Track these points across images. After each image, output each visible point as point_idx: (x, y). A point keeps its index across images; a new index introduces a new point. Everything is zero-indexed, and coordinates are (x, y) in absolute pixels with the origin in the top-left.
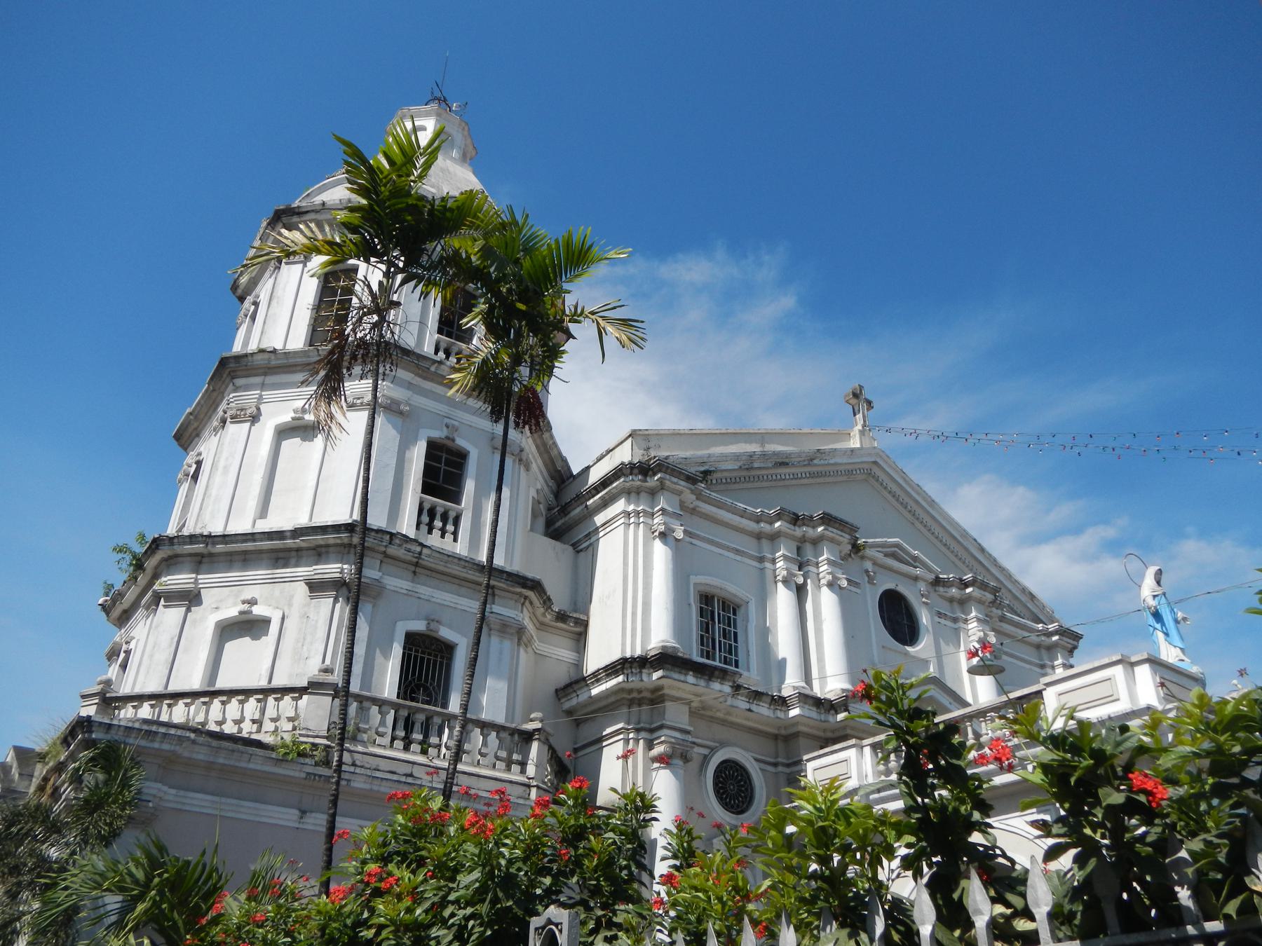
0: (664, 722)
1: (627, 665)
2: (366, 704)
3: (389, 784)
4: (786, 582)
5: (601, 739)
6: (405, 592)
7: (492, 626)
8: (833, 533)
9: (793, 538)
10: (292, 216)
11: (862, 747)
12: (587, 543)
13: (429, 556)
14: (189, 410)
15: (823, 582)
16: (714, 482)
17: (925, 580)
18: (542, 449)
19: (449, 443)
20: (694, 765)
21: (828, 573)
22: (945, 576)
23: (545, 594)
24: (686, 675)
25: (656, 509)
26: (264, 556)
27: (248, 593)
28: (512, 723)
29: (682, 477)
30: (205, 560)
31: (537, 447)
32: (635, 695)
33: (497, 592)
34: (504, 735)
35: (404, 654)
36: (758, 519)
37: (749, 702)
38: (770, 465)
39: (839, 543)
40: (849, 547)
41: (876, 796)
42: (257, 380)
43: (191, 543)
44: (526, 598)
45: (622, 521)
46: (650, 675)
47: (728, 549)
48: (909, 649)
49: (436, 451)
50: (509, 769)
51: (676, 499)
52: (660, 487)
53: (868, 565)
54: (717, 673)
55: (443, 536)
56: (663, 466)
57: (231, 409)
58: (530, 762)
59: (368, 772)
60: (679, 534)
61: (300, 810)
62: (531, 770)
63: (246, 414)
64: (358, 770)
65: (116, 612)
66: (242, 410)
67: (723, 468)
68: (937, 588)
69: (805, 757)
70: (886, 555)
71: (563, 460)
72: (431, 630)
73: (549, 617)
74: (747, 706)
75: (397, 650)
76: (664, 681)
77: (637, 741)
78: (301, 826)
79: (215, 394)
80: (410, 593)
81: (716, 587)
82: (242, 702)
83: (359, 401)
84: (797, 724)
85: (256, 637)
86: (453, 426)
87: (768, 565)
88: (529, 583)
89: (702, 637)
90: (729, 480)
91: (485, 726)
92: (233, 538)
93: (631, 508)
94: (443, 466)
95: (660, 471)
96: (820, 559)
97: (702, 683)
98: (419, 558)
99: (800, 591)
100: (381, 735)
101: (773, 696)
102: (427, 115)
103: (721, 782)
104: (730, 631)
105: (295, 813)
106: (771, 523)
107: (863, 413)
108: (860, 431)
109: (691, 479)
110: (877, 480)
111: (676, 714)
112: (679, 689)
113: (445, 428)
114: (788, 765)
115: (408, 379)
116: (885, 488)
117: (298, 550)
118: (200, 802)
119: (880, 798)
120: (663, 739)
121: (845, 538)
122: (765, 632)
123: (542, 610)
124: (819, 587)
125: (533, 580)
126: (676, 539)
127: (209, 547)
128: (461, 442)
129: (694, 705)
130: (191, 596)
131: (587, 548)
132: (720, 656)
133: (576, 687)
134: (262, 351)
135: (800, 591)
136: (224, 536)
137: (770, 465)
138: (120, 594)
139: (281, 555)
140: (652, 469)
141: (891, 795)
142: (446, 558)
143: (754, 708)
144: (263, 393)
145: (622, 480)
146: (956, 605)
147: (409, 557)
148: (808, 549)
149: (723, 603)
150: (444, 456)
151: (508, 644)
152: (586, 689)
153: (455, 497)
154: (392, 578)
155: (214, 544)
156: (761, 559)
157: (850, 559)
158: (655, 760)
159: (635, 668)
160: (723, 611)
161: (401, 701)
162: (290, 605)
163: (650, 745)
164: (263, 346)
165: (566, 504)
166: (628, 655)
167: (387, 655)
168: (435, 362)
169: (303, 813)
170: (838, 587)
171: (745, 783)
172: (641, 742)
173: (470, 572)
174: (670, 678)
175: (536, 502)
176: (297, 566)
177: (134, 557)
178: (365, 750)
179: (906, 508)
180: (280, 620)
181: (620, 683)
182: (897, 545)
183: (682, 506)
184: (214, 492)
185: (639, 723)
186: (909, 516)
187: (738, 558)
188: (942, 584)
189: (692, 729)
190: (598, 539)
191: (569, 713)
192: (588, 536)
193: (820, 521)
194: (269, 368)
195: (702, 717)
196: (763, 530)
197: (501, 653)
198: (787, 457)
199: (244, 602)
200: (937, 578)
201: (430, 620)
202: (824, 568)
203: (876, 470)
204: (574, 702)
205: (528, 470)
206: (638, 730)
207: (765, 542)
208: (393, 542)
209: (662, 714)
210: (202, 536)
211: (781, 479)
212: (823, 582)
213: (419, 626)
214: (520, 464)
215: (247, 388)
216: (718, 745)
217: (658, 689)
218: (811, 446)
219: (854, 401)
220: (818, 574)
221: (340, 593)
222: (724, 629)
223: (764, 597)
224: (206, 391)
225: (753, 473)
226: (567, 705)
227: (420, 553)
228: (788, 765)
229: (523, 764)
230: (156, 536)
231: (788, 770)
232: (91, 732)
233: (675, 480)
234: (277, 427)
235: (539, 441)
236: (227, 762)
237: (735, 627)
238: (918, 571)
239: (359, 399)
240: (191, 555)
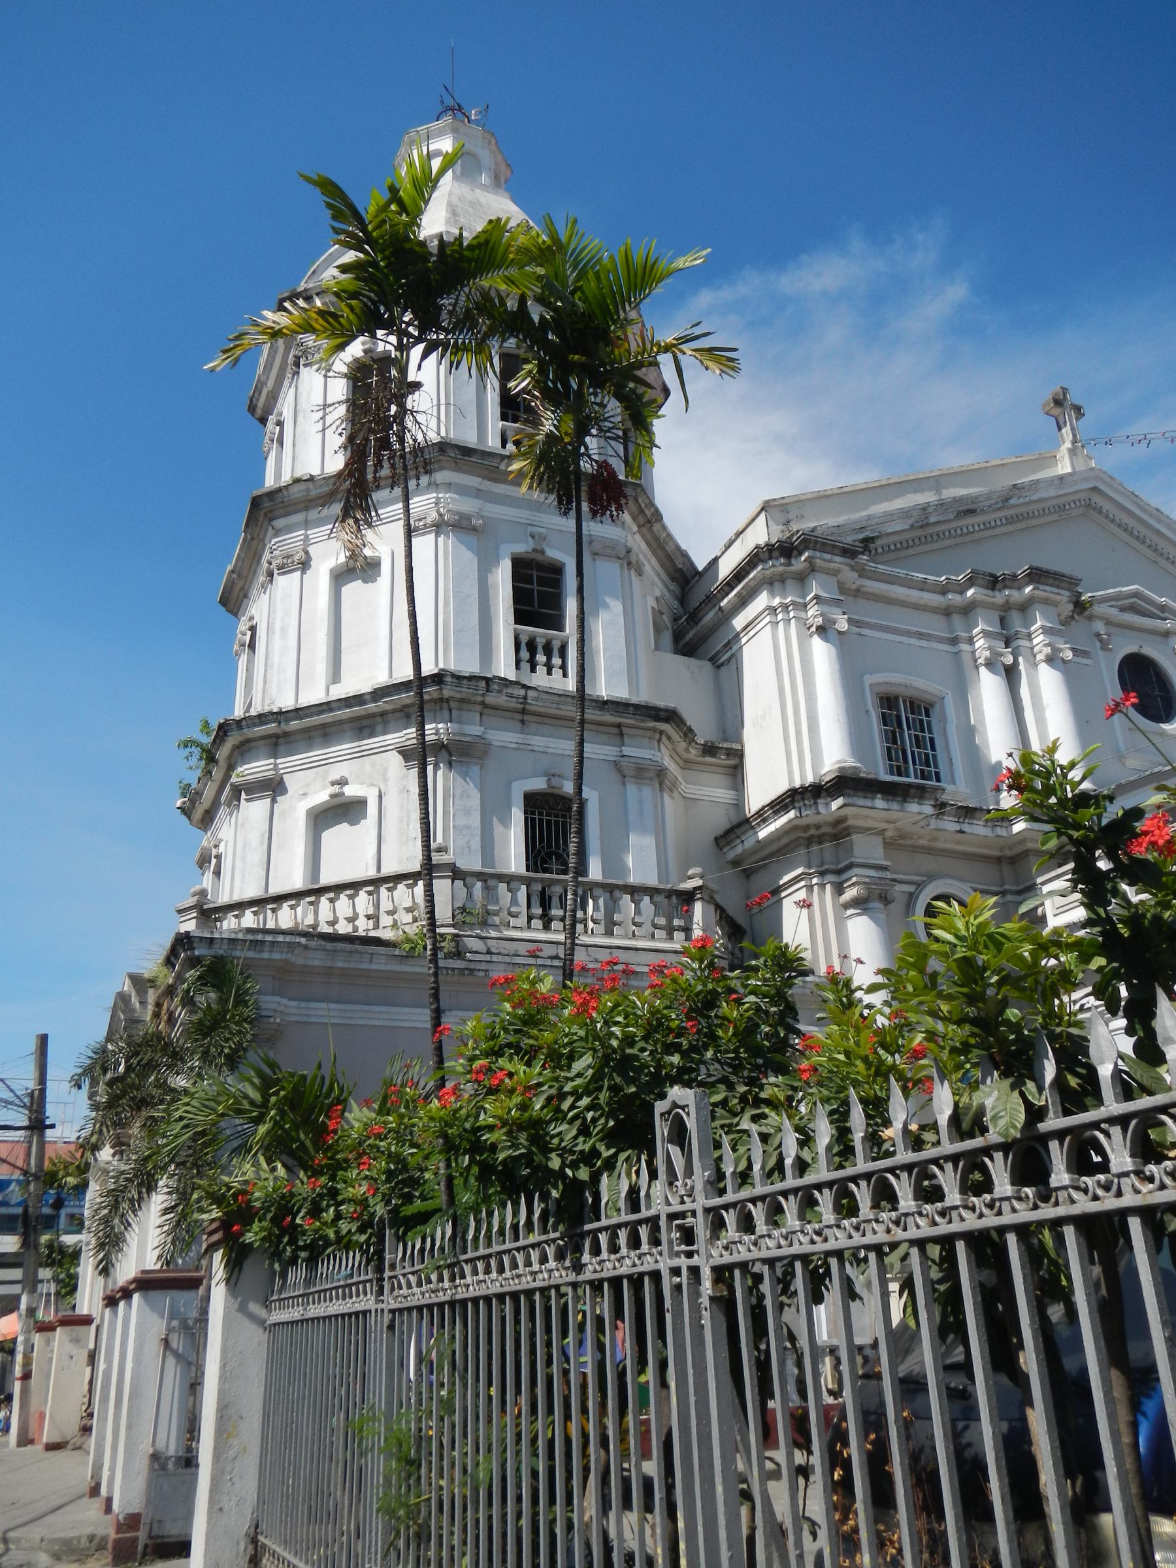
0: (853, 860)
1: (798, 797)
2: (491, 882)
4: (989, 665)
5: (777, 891)
6: (515, 746)
7: (626, 772)
8: (1045, 592)
9: (992, 606)
13: (536, 699)
14: (229, 568)
15: (1040, 657)
16: (880, 550)
18: (655, 545)
20: (897, 907)
21: (1046, 645)
23: (685, 724)
24: (873, 799)
25: (808, 598)
26: (346, 726)
27: (336, 772)
28: (668, 883)
29: (837, 551)
30: (281, 741)
31: (648, 543)
32: (812, 832)
33: (625, 730)
34: (659, 898)
35: (526, 819)
36: (943, 590)
38: (952, 516)
39: (1055, 604)
40: (1071, 607)
42: (298, 517)
43: (262, 724)
44: (661, 732)
45: (768, 619)
46: (827, 805)
47: (909, 634)
48: (1166, 727)
49: (523, 569)
50: (671, 938)
51: (832, 581)
53: (1100, 627)
54: (912, 791)
55: (549, 673)
56: (809, 541)
57: (276, 557)
58: (695, 926)
59: (507, 959)
60: (843, 625)
62: (697, 933)
63: (293, 562)
64: (495, 958)
65: (198, 814)
66: (288, 557)
67: (890, 531)
69: (1039, 880)
70: (1123, 609)
73: (693, 751)
74: (957, 827)
75: (518, 816)
76: (848, 811)
77: (822, 886)
79: (254, 543)
81: (900, 685)
82: (351, 897)
83: (421, 523)
84: (1024, 841)
85: (354, 822)
86: (540, 535)
87: (964, 647)
88: (662, 714)
89: (889, 749)
90: (899, 546)
91: (635, 891)
92: (307, 711)
93: (776, 601)
94: (535, 587)
95: (807, 548)
96: (1033, 628)
97: (895, 806)
98: (525, 703)
99: (1011, 674)
100: (515, 915)
102: (441, 133)
104: (924, 737)
106: (962, 592)
107: (1071, 425)
108: (1069, 450)
109: (848, 552)
110: (1100, 512)
111: (866, 849)
112: (866, 817)
113: (530, 539)
115: (476, 485)
116: (1113, 521)
117: (383, 714)
118: (323, 1012)
120: (854, 880)
121: (1063, 597)
122: (970, 733)
123: (684, 745)
124: (1036, 665)
125: (667, 710)
126: (840, 633)
127: (283, 724)
129: (888, 834)
131: (729, 660)
132: (915, 770)
133: (738, 832)
134: (297, 481)
135: (1011, 674)
136: (297, 710)
137: (952, 516)
138: (197, 793)
139: (365, 723)
140: (796, 548)
142: (557, 698)
143: (966, 828)
144: (309, 532)
145: (760, 567)
147: (513, 704)
148: (1015, 618)
149: (912, 703)
150: (535, 573)
151: (647, 792)
152: (751, 832)
153: (556, 623)
155: (287, 721)
156: (954, 641)
157: (1073, 623)
158: (846, 906)
160: (913, 713)
161: (531, 874)
162: (385, 780)
163: (839, 890)
164: (297, 475)
165: (695, 609)
166: (797, 784)
167: (506, 822)
168: (503, 457)
170: (1060, 662)
172: (828, 887)
174: (854, 805)
175: (657, 613)
176: (384, 733)
177: (203, 750)
178: (499, 935)
179: (1144, 542)
180: (377, 800)
181: (791, 820)
182: (1136, 594)
183: (842, 588)
184: (275, 660)
185: (822, 865)
186: (1150, 554)
187: (924, 643)
189: (889, 863)
190: (741, 648)
191: (735, 863)
192: (728, 645)
193: (1027, 579)
194: (310, 501)
195: (901, 847)
196: (952, 603)
197: (641, 802)
198: (973, 503)
199: (333, 784)
201: (550, 776)
202: (1039, 639)
203: (1097, 500)
204: (739, 850)
205: (640, 575)
206: (821, 874)
207: (957, 619)
209: (850, 851)
210: (272, 713)
211: (969, 533)
212: (1040, 657)
213: (538, 784)
214: (629, 569)
215: (290, 529)
217: (840, 821)
218: (1004, 482)
219: (1057, 411)
220: (1032, 648)
222: (916, 737)
223: (963, 688)
224: (244, 541)
225: (930, 530)
227: (525, 697)
229: (687, 930)
230: (222, 721)
232: (193, 949)
233: (827, 556)
234: (331, 571)
235: (649, 536)
236: (346, 965)
237: (930, 732)
239: (420, 520)
240: (264, 738)
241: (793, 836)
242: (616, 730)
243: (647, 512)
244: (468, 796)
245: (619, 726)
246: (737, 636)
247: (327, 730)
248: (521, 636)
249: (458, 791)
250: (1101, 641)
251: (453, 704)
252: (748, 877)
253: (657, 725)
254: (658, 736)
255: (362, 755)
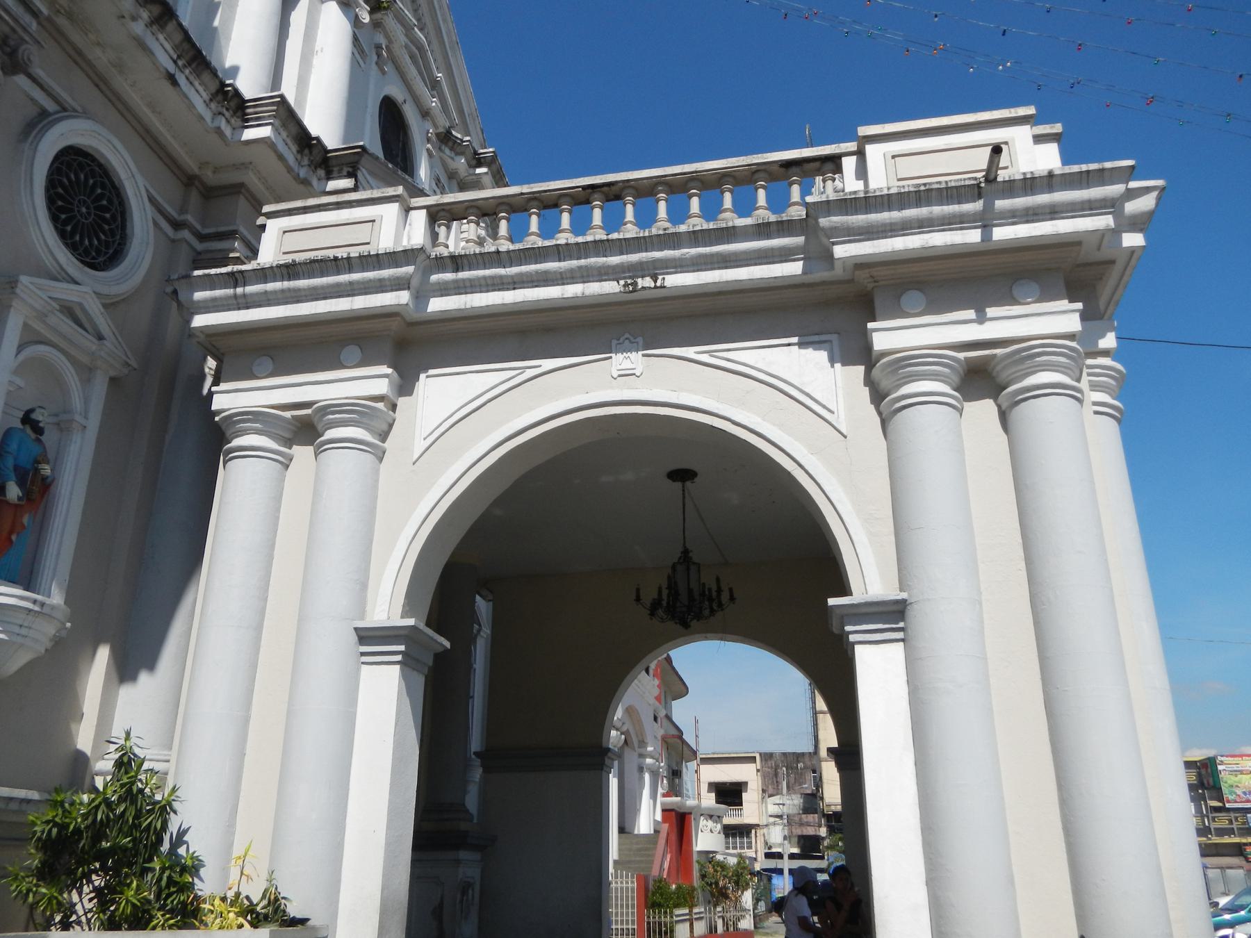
11: (408, 210)
17: (435, 126)
22: (459, 136)
37: (175, 62)
41: (449, 276)
68: (443, 147)
74: (171, 68)
84: (245, 166)
101: (223, 85)
103: (61, 197)
114: (202, 238)
119: (456, 281)
141: (485, 278)
143: (181, 79)
146: (454, 182)
171: (114, 218)
188: (450, 144)
200: (448, 133)
216: (79, 109)
228: (202, 238)
231: (199, 246)
238: (434, 103)
250: (379, 55)
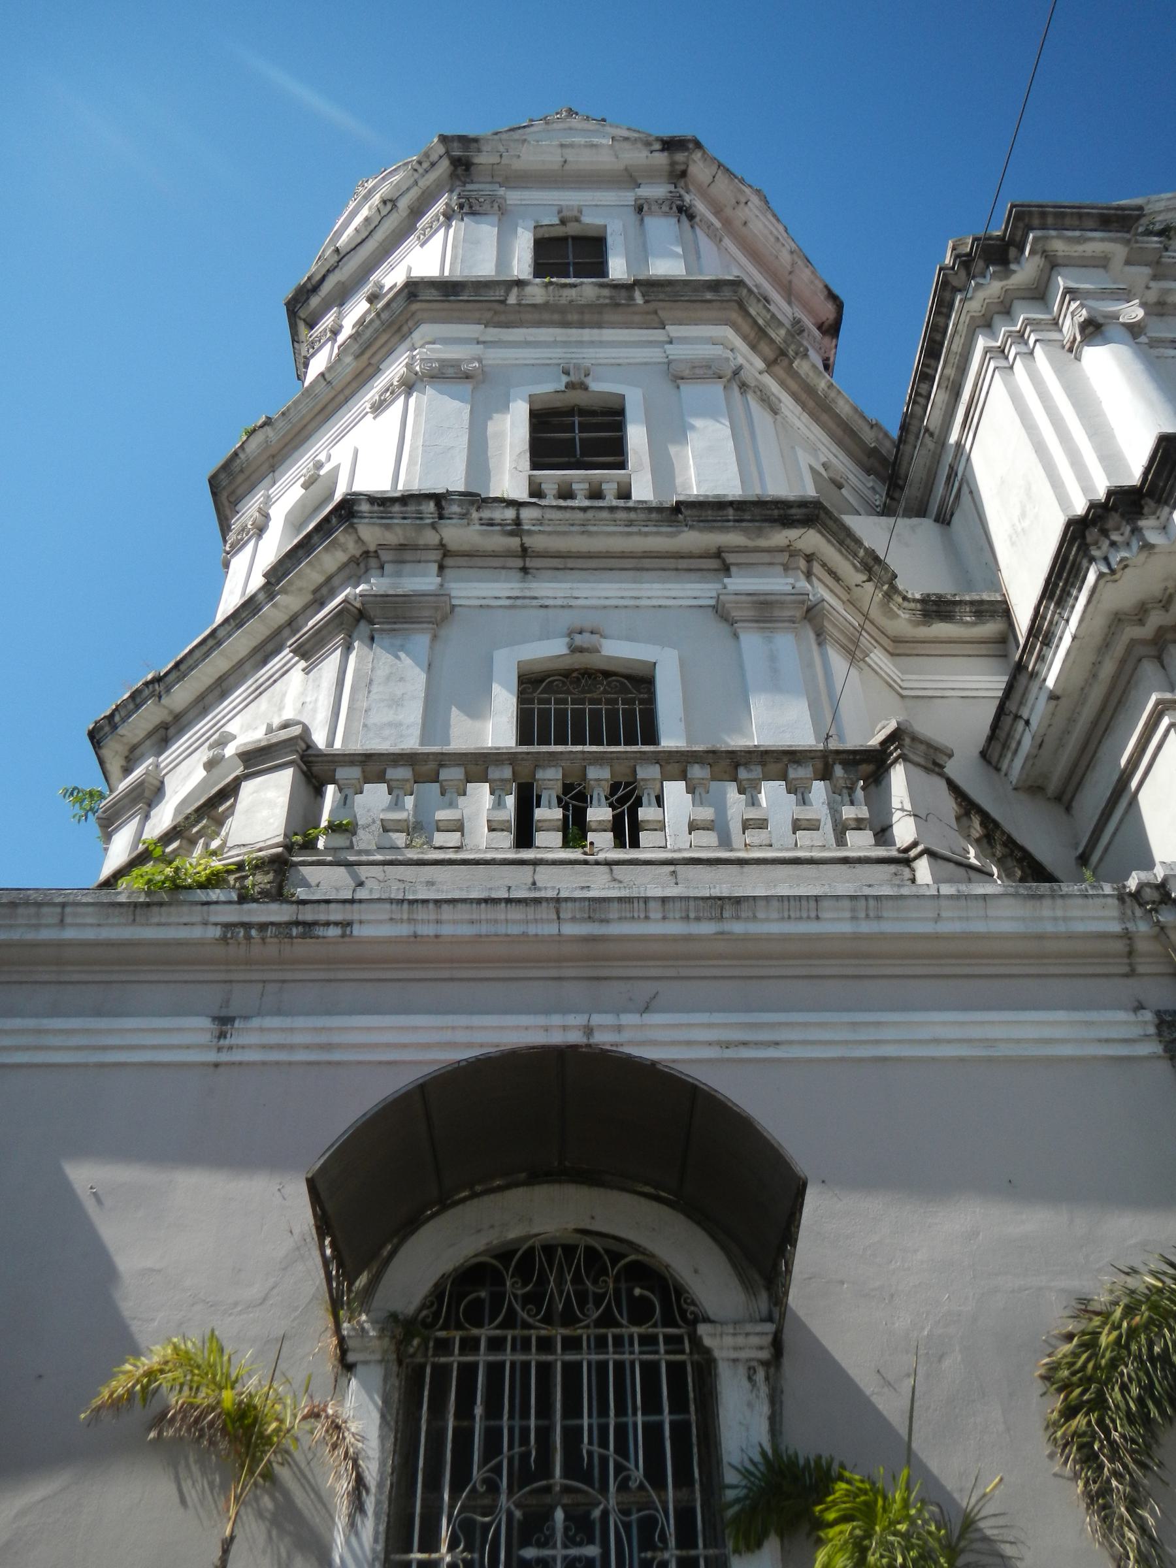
1: (1092, 534)
3: (463, 912)
5: (1125, 777)
6: (508, 602)
7: (735, 614)
10: (308, 298)
12: (957, 485)
13: (540, 522)
18: (811, 404)
19: (576, 398)
23: (858, 542)
29: (1091, 223)
30: (172, 731)
33: (731, 558)
34: (795, 773)
52: (1048, 266)
58: (897, 816)
60: (1133, 312)
61: (215, 1019)
62: (904, 831)
66: (243, 530)
71: (872, 426)
72: (581, 650)
73: (904, 615)
78: (224, 1057)
80: (519, 602)
92: (190, 661)
95: (1030, 228)
105: (199, 1027)
127: (164, 701)
128: (601, 386)
130: (147, 794)
133: (1012, 706)
154: (476, 585)
155: (168, 690)
159: (1117, 529)
166: (1080, 507)
169: (224, 1022)
173: (646, 529)
194: (273, 456)
197: (773, 658)
204: (1027, 743)
208: (446, 512)
221: (355, 635)
226: (1016, 766)
227: (518, 522)
230: (91, 726)
235: (794, 386)
241: (1119, 649)
242: (714, 564)
243: (773, 335)
244: (402, 679)
245: (718, 554)
246: (959, 445)
247: (224, 685)
248: (543, 486)
249: (381, 673)
251: (385, 556)
252: (1068, 809)
253: (792, 534)
254: (802, 563)
255: (259, 692)
